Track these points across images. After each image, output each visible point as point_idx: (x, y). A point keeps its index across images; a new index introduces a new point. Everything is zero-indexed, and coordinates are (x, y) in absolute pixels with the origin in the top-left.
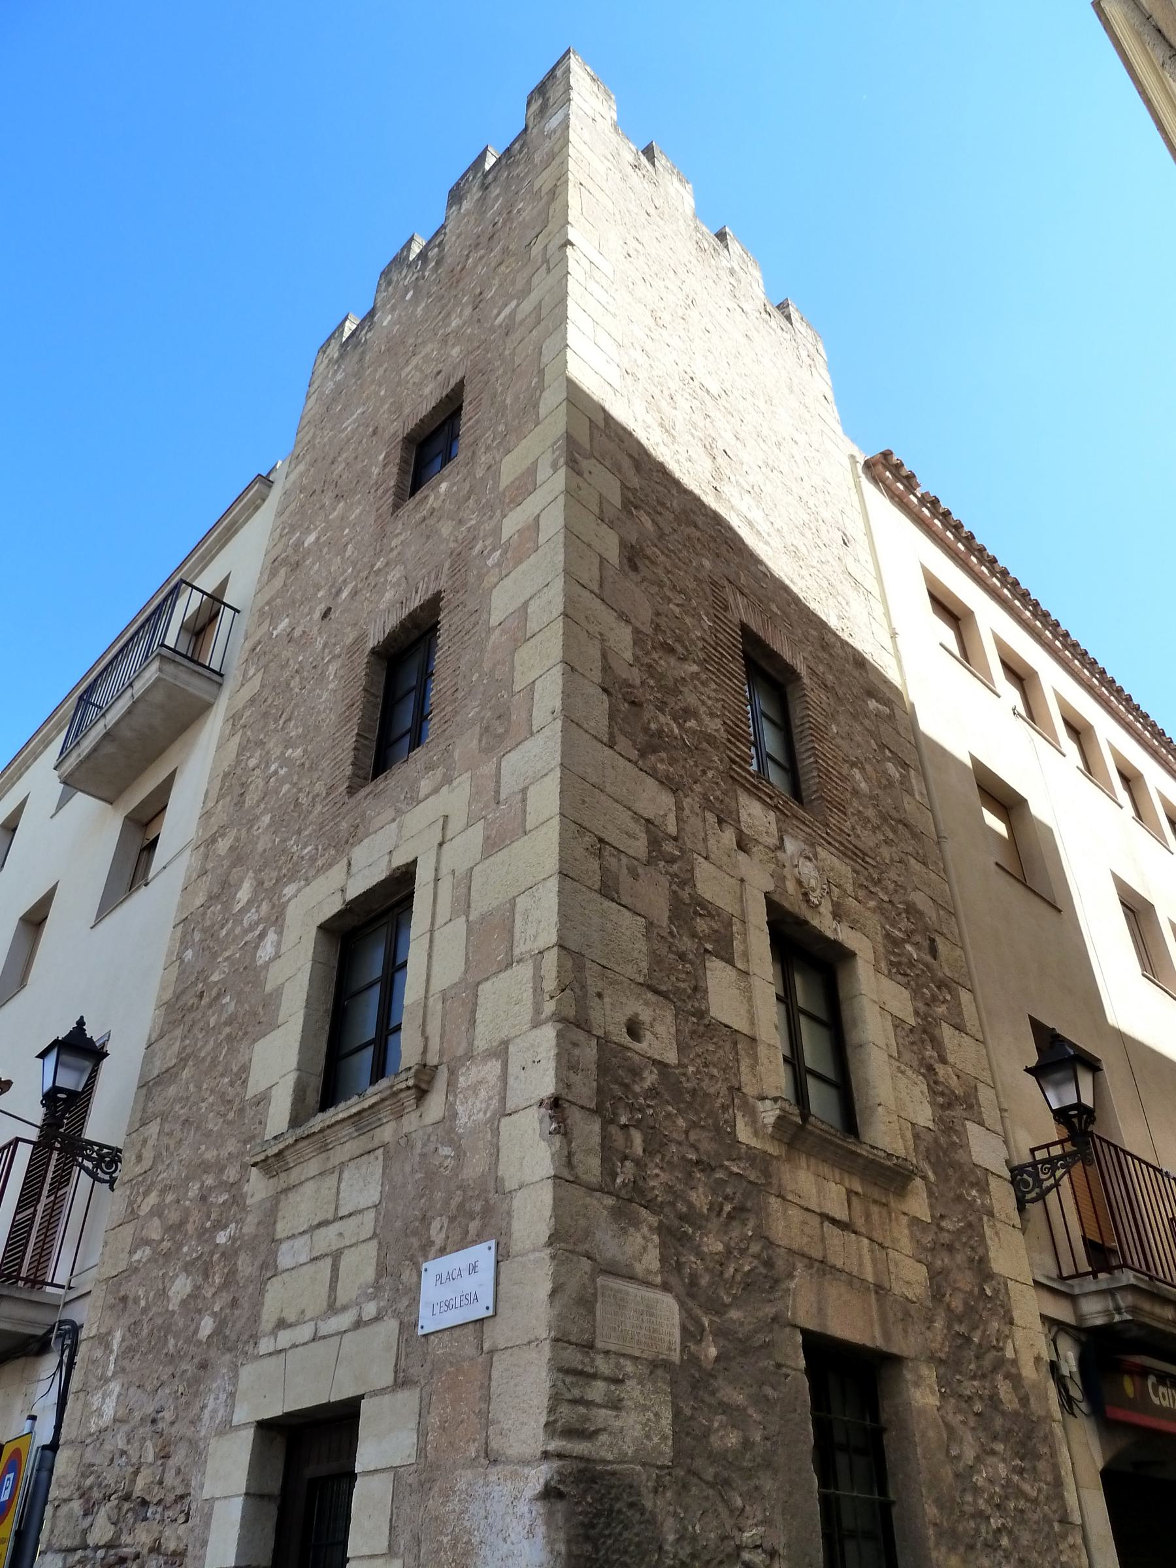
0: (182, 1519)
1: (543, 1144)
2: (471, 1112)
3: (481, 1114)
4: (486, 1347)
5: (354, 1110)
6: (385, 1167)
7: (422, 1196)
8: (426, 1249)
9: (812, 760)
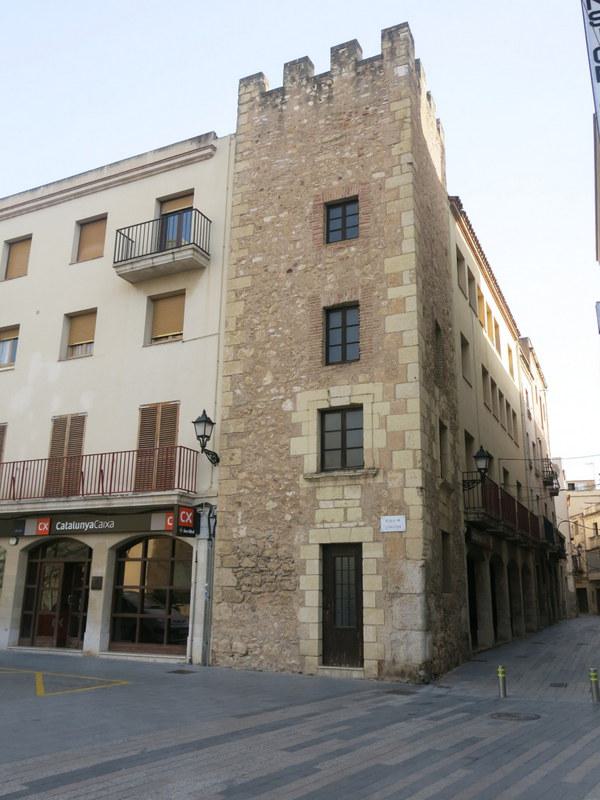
2: (393, 484)
8: (380, 513)
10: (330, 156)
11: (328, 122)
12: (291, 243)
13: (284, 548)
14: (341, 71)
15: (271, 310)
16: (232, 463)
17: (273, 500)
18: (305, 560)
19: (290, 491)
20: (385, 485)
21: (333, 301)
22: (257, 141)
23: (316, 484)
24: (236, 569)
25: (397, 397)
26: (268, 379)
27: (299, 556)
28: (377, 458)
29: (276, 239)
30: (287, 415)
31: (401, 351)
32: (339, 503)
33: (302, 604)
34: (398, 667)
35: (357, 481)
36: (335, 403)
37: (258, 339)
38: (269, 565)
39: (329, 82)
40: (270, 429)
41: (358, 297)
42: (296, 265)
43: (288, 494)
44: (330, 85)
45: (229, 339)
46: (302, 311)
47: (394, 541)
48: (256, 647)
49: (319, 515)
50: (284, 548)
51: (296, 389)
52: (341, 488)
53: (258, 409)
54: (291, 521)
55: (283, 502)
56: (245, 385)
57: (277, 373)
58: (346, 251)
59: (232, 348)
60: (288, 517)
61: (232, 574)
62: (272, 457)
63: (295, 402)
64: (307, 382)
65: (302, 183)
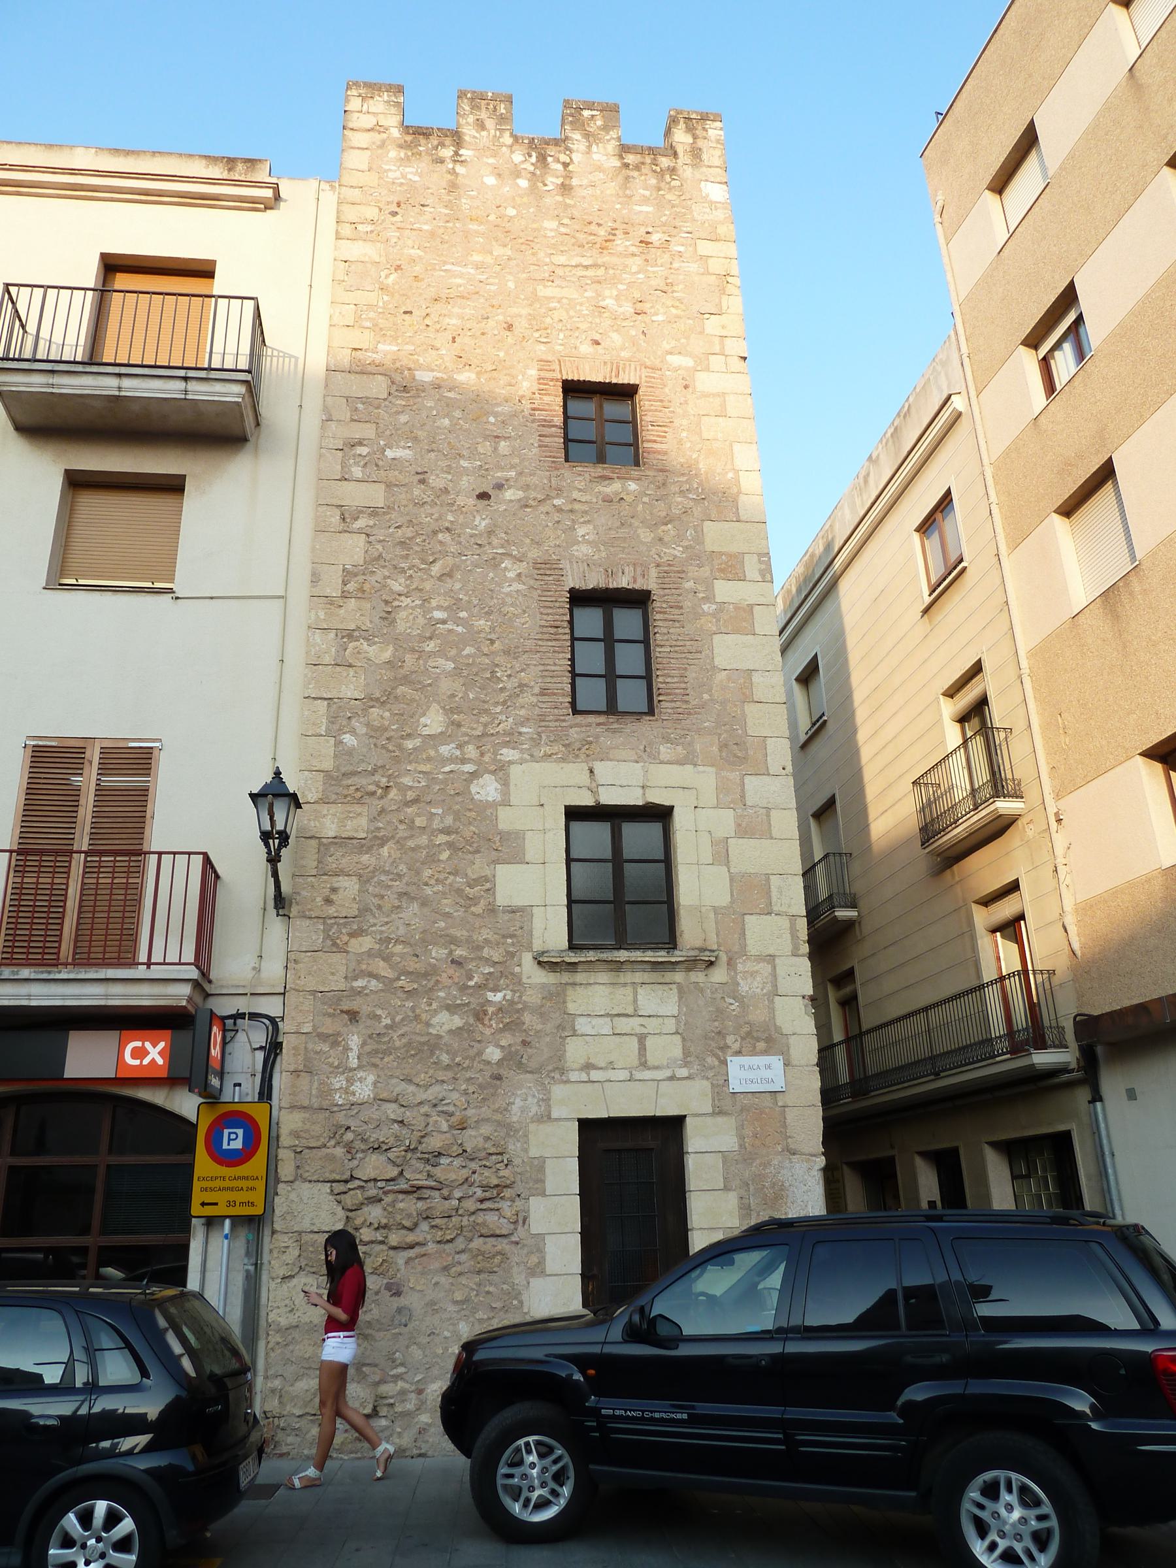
8: (724, 1048)
10: (571, 293)
11: (563, 230)
12: (486, 438)
13: (486, 1130)
14: (589, 147)
15: (436, 569)
16: (332, 911)
17: (451, 1009)
18: (542, 1160)
19: (495, 990)
20: (731, 989)
21: (593, 580)
22: (394, 214)
23: (566, 977)
24: (342, 1184)
25: (749, 803)
26: (433, 721)
27: (526, 1151)
28: (711, 926)
29: (446, 422)
30: (485, 810)
31: (750, 709)
32: (624, 1025)
33: (538, 1270)
35: (669, 976)
36: (610, 797)
37: (401, 626)
38: (437, 1172)
39: (563, 158)
40: (441, 839)
41: (650, 583)
42: (499, 487)
43: (490, 996)
44: (566, 165)
45: (322, 615)
46: (516, 586)
47: (758, 1113)
48: (403, 1392)
49: (575, 1051)
50: (486, 1130)
51: (508, 754)
52: (629, 990)
53: (404, 789)
54: (500, 1063)
55: (480, 1015)
56: (368, 725)
57: (457, 710)
58: (616, 486)
59: (332, 635)
60: (493, 1054)
61: (328, 1202)
62: (447, 905)
63: (505, 783)
64: (536, 742)
65: (510, 327)
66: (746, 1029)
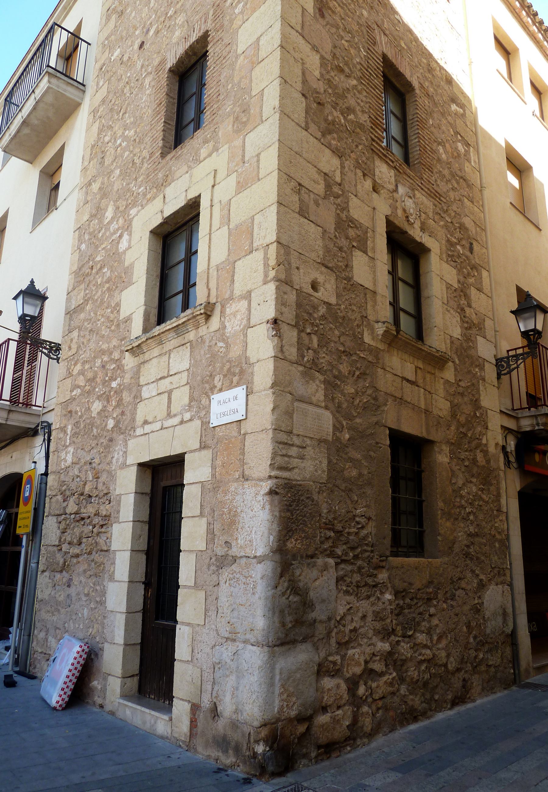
0: (107, 502)
1: (269, 341)
2: (233, 326)
3: (238, 327)
4: (242, 432)
5: (174, 325)
6: (191, 352)
7: (210, 366)
8: (212, 389)
9: (417, 140)
18: (121, 495)
34: (221, 725)
47: (223, 441)
66: (227, 366)
